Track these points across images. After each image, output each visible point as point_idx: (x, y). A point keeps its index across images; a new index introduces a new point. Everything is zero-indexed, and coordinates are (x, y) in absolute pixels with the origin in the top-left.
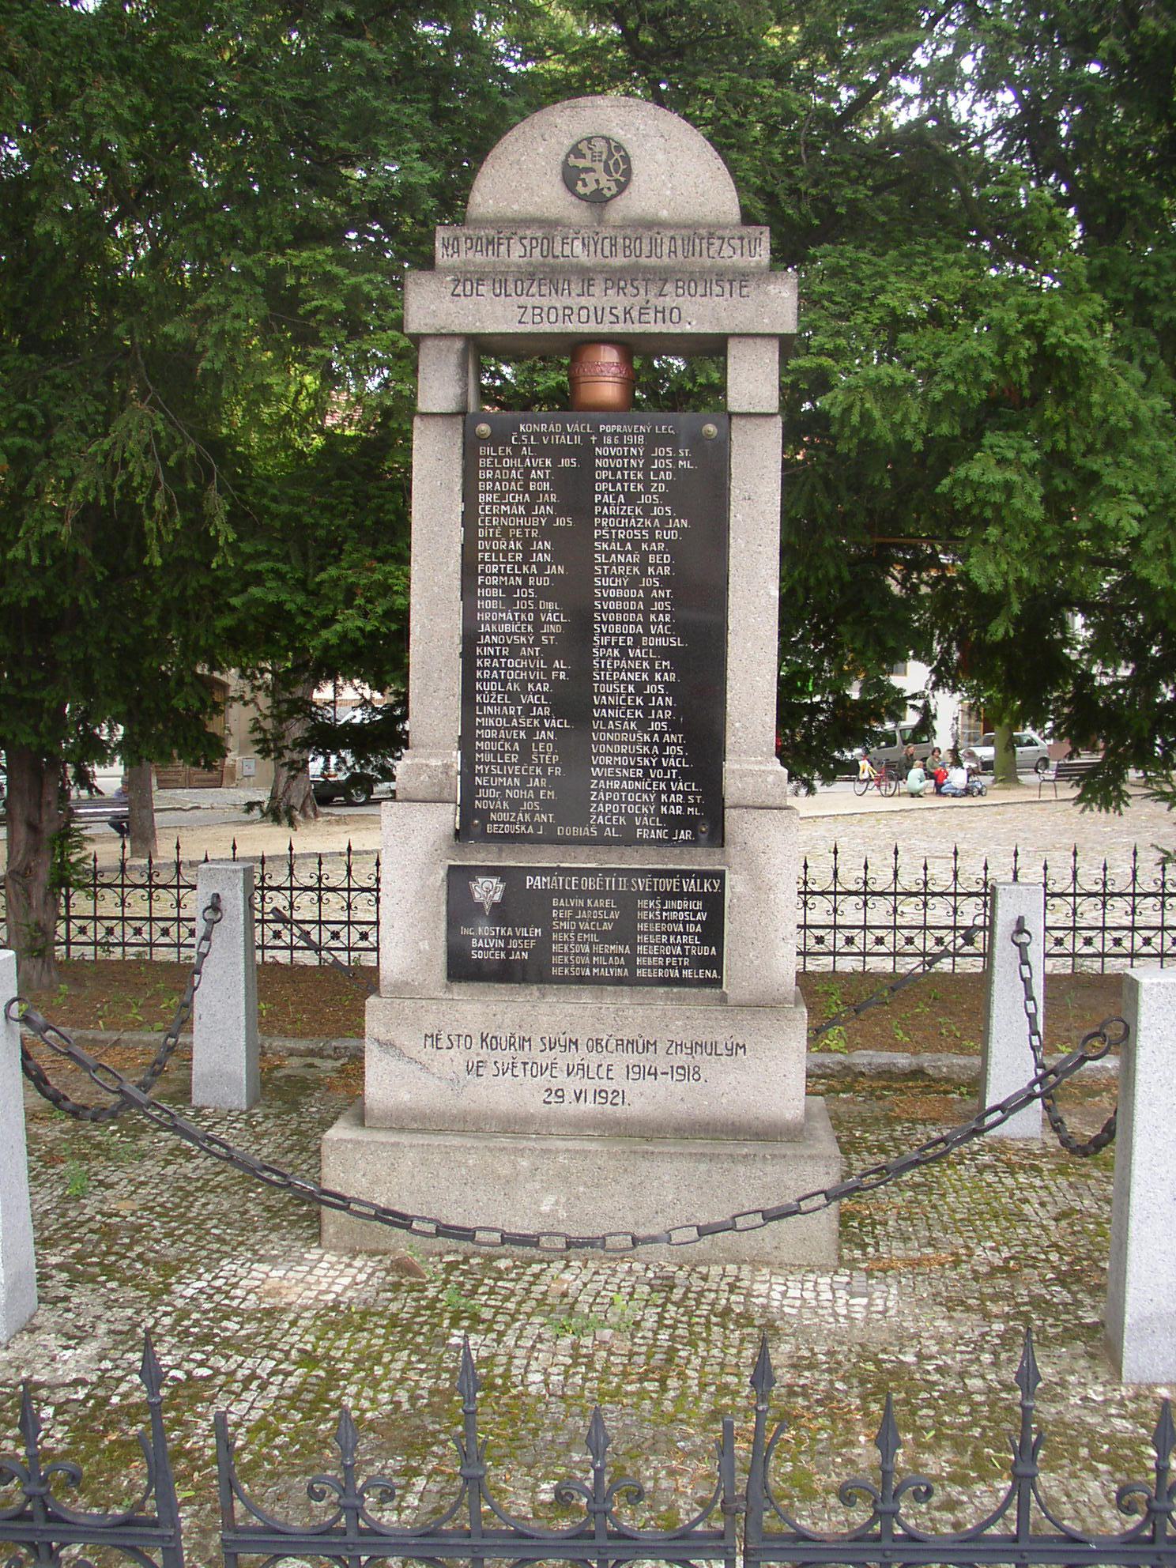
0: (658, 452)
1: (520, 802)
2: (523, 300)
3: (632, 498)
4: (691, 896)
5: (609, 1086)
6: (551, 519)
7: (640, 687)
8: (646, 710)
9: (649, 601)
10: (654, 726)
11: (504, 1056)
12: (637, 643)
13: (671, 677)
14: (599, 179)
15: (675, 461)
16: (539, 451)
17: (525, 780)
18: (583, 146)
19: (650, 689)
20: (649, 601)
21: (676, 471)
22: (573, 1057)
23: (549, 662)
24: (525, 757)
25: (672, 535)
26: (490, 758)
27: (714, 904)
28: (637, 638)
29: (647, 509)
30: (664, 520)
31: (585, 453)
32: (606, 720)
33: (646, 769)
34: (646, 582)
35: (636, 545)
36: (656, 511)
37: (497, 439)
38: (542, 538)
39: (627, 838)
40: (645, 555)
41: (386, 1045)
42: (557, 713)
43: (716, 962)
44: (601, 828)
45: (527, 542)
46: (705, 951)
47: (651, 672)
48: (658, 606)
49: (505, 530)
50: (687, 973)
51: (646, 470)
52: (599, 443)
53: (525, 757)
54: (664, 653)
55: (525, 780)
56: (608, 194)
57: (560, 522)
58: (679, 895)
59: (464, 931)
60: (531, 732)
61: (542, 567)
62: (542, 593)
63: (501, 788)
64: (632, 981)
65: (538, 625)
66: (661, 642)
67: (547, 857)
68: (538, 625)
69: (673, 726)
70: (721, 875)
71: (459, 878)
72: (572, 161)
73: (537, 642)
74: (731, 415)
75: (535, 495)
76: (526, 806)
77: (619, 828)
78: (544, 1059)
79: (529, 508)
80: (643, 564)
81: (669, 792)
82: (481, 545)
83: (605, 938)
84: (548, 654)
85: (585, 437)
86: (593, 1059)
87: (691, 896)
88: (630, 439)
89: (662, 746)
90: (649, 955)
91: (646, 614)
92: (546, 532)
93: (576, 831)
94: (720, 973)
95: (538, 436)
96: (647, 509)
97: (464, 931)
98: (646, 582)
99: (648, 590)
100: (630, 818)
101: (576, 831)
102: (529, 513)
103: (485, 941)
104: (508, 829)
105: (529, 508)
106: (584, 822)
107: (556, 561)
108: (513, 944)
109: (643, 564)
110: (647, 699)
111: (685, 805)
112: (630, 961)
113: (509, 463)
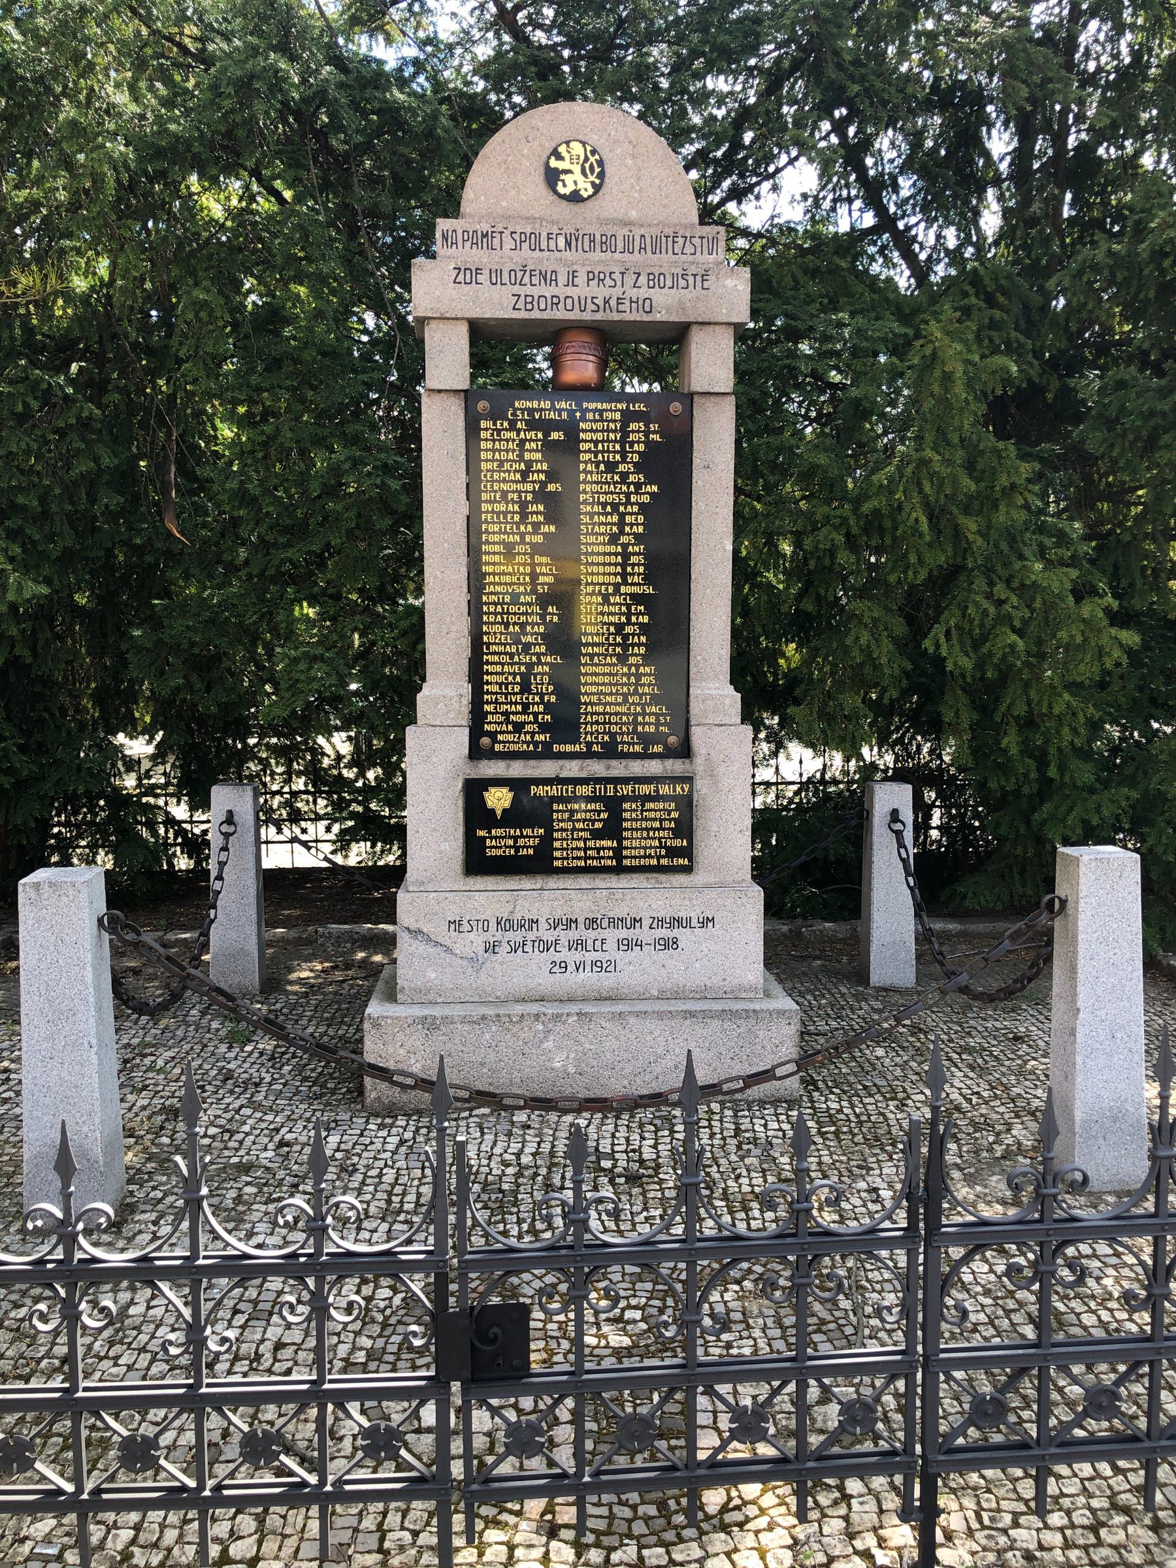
0: (633, 426)
1: (523, 724)
2: (517, 289)
3: (611, 467)
4: (664, 798)
5: (604, 957)
6: (544, 485)
7: (619, 628)
8: (625, 646)
9: (626, 556)
10: (632, 660)
11: (517, 936)
12: (617, 591)
13: (646, 619)
14: (575, 181)
15: (647, 433)
16: (532, 425)
17: (526, 706)
18: (562, 149)
19: (628, 629)
20: (626, 556)
21: (647, 443)
22: (573, 934)
23: (544, 608)
24: (525, 688)
25: (645, 499)
26: (496, 688)
27: (687, 805)
28: (617, 586)
29: (624, 476)
30: (638, 486)
31: (572, 430)
32: (592, 656)
33: (625, 696)
34: (624, 539)
35: (616, 507)
36: (632, 478)
37: (494, 417)
38: (535, 501)
39: (611, 751)
40: (622, 516)
41: (416, 933)
42: (551, 651)
43: (687, 852)
44: (589, 745)
45: (523, 505)
46: (678, 843)
47: (629, 615)
48: (634, 559)
49: (504, 494)
50: (664, 862)
51: (623, 442)
52: (585, 420)
53: (525, 688)
54: (637, 598)
55: (526, 706)
56: (585, 194)
57: (551, 487)
58: (656, 798)
59: (481, 833)
60: (530, 666)
61: (536, 526)
62: (536, 549)
63: (506, 714)
64: (619, 870)
65: (534, 576)
66: (635, 589)
67: (547, 768)
68: (534, 576)
69: (647, 659)
70: (689, 780)
71: (474, 790)
72: (554, 163)
73: (534, 591)
74: (691, 395)
75: (529, 464)
76: (528, 728)
77: (604, 745)
78: (549, 936)
79: (525, 475)
80: (621, 524)
81: (644, 714)
82: (484, 507)
83: (597, 835)
84: (544, 601)
85: (571, 413)
86: (592, 934)
87: (664, 798)
88: (609, 415)
89: (638, 676)
90: (636, 845)
91: (624, 565)
92: (541, 495)
93: (569, 748)
94: (691, 860)
95: (531, 411)
96: (624, 476)
97: (481, 833)
98: (624, 539)
99: (625, 546)
100: (613, 736)
101: (569, 748)
102: (524, 479)
103: (498, 843)
104: (513, 748)
105: (525, 475)
106: (575, 740)
107: (549, 520)
108: (521, 842)
109: (621, 524)
110: (626, 637)
111: (657, 724)
112: (618, 853)
113: (508, 435)
